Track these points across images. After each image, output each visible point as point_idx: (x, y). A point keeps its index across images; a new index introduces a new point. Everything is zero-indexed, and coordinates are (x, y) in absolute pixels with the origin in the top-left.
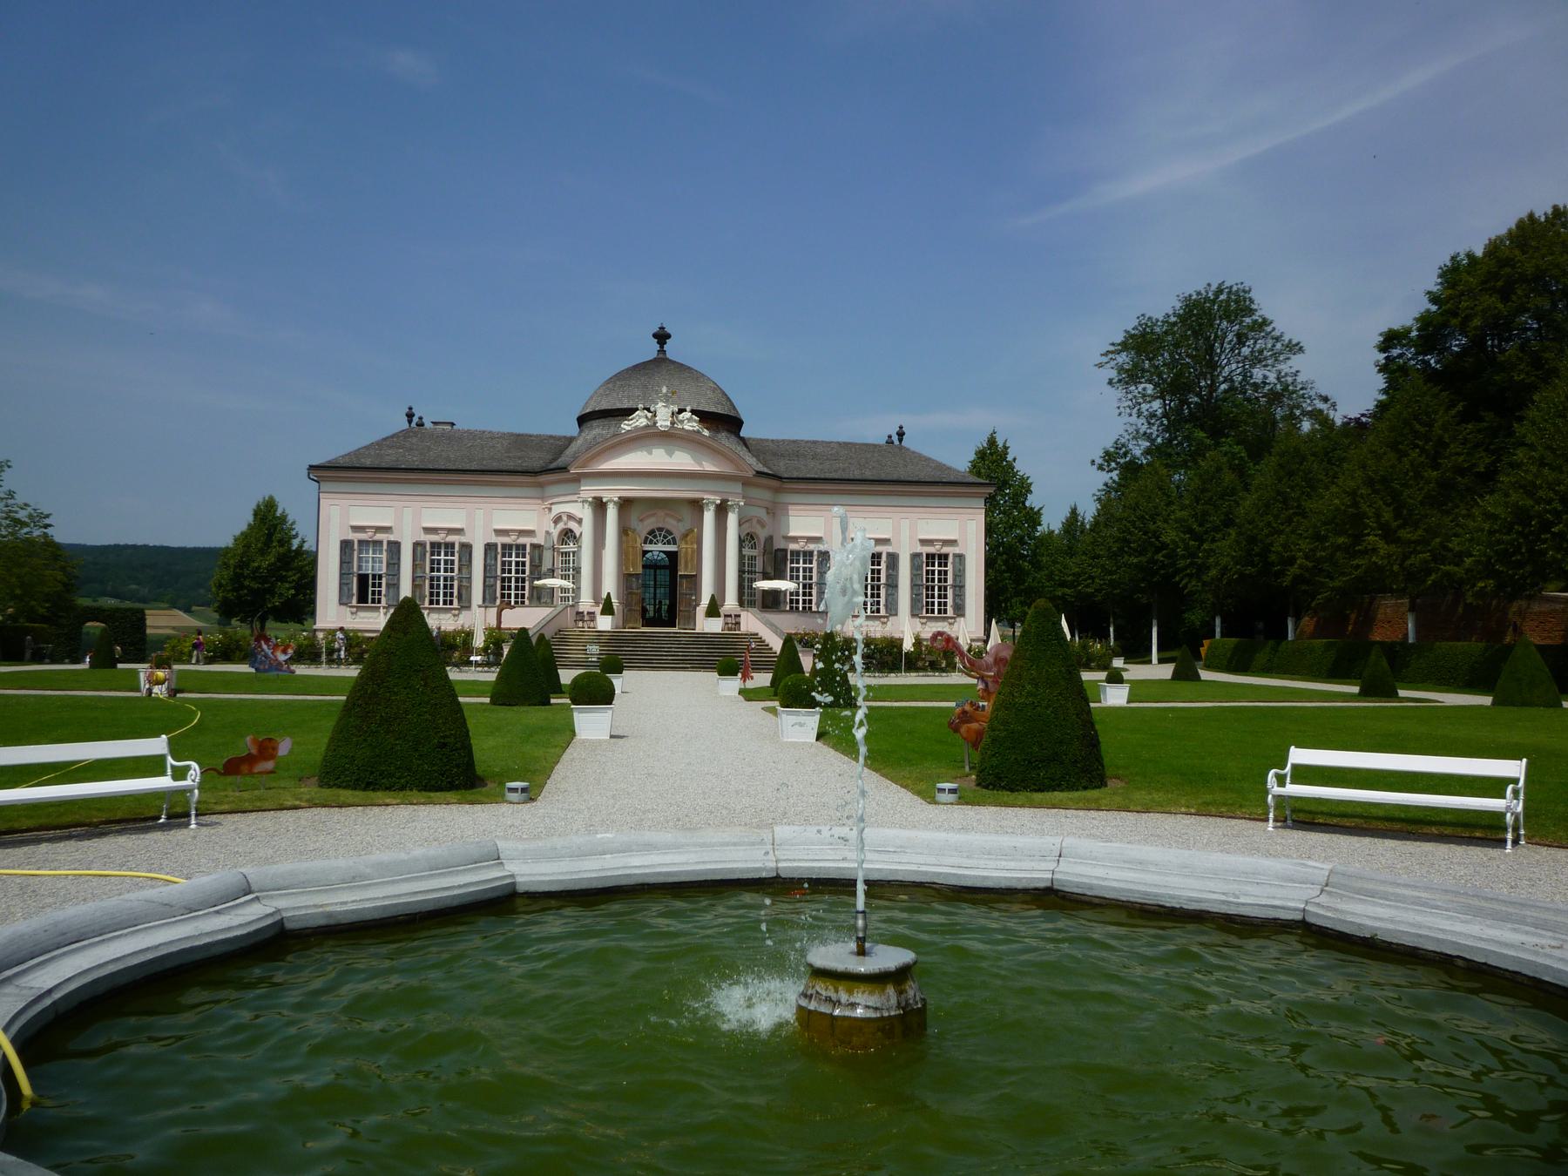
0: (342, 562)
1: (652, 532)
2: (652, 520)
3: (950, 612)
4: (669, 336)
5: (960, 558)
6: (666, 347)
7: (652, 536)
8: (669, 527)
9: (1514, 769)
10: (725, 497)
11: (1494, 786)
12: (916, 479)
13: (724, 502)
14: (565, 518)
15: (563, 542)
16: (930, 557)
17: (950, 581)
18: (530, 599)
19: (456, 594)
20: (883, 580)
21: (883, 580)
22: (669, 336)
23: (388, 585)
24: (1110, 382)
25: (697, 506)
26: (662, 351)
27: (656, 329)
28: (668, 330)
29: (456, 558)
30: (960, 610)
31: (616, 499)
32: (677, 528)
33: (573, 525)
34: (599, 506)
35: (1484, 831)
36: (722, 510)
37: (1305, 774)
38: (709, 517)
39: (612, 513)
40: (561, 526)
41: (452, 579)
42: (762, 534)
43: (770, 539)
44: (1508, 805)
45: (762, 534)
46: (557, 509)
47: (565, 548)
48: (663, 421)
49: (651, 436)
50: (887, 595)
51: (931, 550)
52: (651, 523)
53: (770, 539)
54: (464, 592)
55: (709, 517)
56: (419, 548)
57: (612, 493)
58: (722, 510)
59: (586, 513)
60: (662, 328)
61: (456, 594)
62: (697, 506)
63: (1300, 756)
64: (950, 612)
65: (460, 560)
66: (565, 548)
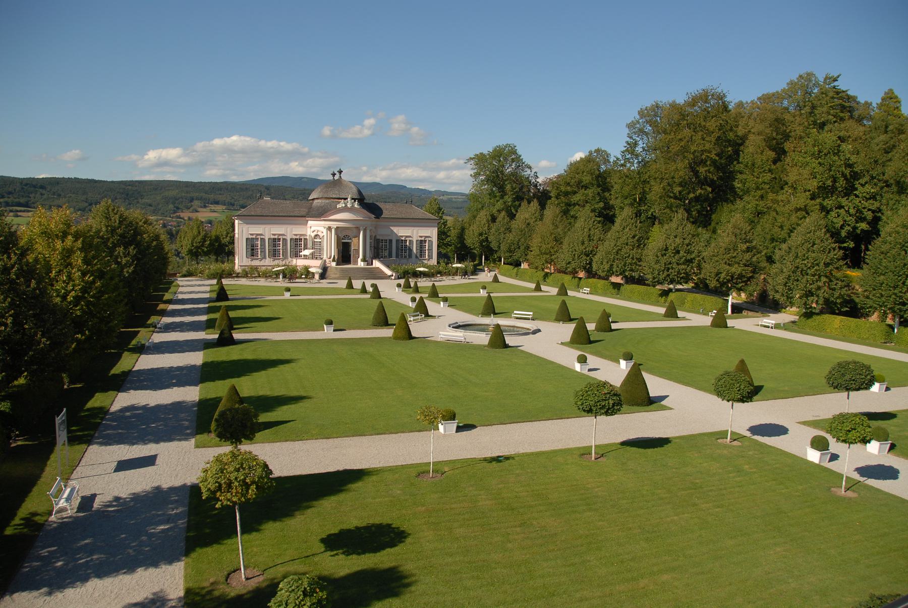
9: (532, 313)
11: (529, 315)
15: (315, 238)
24: (471, 175)
29: (281, 243)
34: (329, 229)
35: (528, 319)
37: (515, 314)
40: (315, 233)
43: (375, 236)
46: (313, 229)
47: (315, 240)
48: (349, 205)
49: (345, 209)
53: (375, 236)
57: (334, 225)
59: (325, 231)
63: (515, 312)
66: (315, 240)
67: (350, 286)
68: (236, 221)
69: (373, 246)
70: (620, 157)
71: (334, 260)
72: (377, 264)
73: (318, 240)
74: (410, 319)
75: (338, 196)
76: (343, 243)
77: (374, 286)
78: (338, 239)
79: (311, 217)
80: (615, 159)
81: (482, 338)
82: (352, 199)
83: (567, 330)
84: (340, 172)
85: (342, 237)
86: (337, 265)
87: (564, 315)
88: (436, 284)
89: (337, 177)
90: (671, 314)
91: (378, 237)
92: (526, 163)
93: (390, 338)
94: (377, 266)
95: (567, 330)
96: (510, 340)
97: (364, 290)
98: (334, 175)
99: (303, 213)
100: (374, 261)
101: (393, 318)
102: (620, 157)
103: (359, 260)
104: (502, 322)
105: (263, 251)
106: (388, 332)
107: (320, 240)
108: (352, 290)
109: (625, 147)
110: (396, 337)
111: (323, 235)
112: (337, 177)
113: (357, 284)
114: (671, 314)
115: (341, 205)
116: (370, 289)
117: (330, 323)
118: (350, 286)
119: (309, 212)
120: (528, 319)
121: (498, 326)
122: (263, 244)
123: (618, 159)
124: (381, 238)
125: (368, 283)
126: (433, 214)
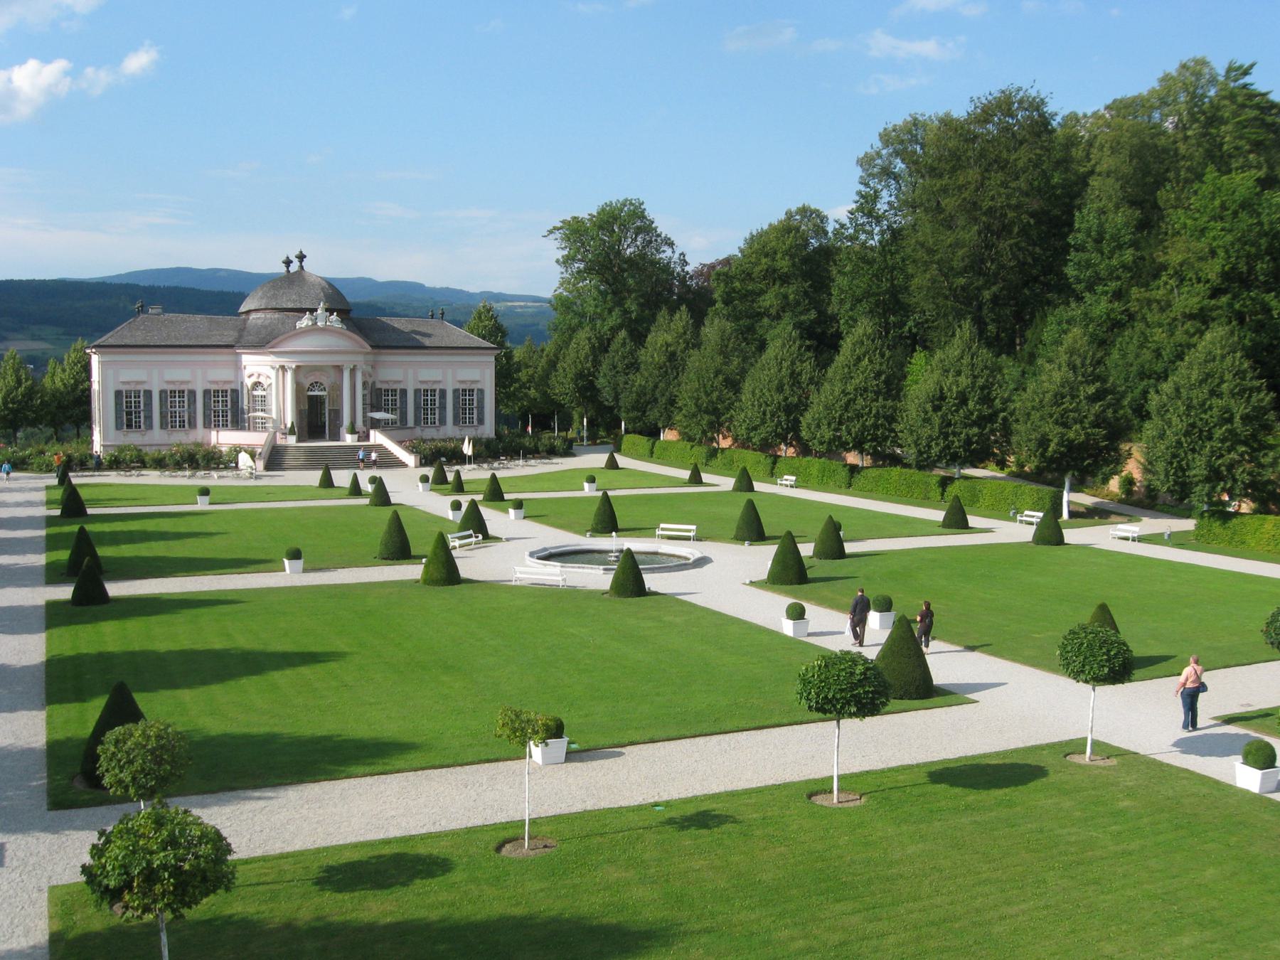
0: (116, 404)
1: (311, 384)
2: (312, 377)
3: (475, 423)
4: (305, 257)
5: (481, 391)
6: (303, 264)
7: (313, 386)
8: (321, 381)
9: (694, 527)
10: (355, 363)
12: (455, 345)
13: (355, 366)
14: (256, 375)
16: (464, 390)
17: (475, 404)
18: (232, 422)
19: (186, 421)
20: (437, 405)
21: (437, 405)
22: (305, 257)
23: (145, 417)
24: (557, 261)
25: (339, 369)
26: (302, 267)
27: (298, 253)
28: (304, 253)
29: (186, 399)
30: (481, 421)
31: (294, 367)
32: (326, 381)
33: (262, 380)
35: (688, 539)
36: (353, 371)
37: (663, 529)
38: (346, 375)
39: (289, 376)
40: (254, 379)
41: (183, 411)
42: (370, 381)
43: (374, 383)
44: (691, 534)
45: (370, 381)
49: (313, 329)
50: (440, 414)
51: (464, 386)
52: (311, 379)
53: (374, 383)
54: (192, 421)
55: (346, 375)
56: (163, 395)
58: (353, 371)
59: (273, 373)
60: (301, 252)
61: (186, 421)
62: (339, 369)
64: (475, 423)
65: (189, 400)
66: (255, 393)
67: (327, 482)
68: (95, 360)
69: (368, 401)
70: (846, 221)
71: (292, 432)
72: (377, 437)
73: (259, 393)
74: (454, 543)
75: (298, 306)
76: (311, 398)
77: (378, 482)
78: (299, 390)
79: (244, 347)
80: (837, 226)
81: (598, 578)
82: (327, 310)
83: (762, 557)
84: (301, 257)
85: (307, 386)
86: (299, 440)
87: (752, 530)
88: (499, 474)
89: (294, 267)
90: (957, 521)
91: (379, 386)
92: (663, 236)
93: (417, 581)
94: (378, 442)
95: (762, 557)
96: (652, 581)
97: (356, 490)
98: (288, 263)
99: (229, 341)
100: (372, 432)
101: (421, 543)
102: (846, 221)
103: (343, 430)
104: (636, 544)
105: (149, 418)
106: (412, 571)
107: (264, 393)
108: (330, 490)
109: (856, 202)
110: (429, 580)
111: (269, 381)
112: (294, 267)
113: (342, 478)
114: (957, 521)
115: (305, 322)
116: (368, 488)
117: (295, 555)
118: (327, 482)
119: (240, 336)
120: (688, 539)
121: (629, 554)
122: (149, 404)
123: (842, 226)
124: (384, 386)
125: (364, 476)
126: (484, 338)
